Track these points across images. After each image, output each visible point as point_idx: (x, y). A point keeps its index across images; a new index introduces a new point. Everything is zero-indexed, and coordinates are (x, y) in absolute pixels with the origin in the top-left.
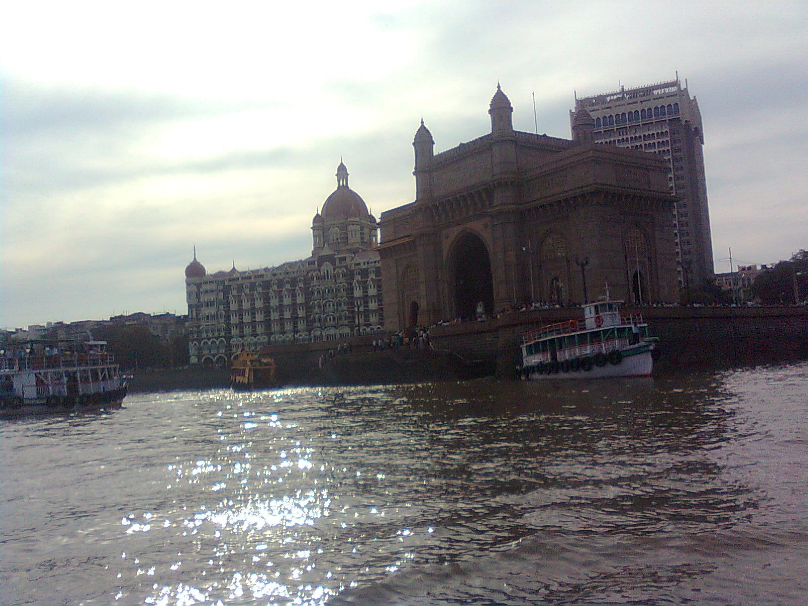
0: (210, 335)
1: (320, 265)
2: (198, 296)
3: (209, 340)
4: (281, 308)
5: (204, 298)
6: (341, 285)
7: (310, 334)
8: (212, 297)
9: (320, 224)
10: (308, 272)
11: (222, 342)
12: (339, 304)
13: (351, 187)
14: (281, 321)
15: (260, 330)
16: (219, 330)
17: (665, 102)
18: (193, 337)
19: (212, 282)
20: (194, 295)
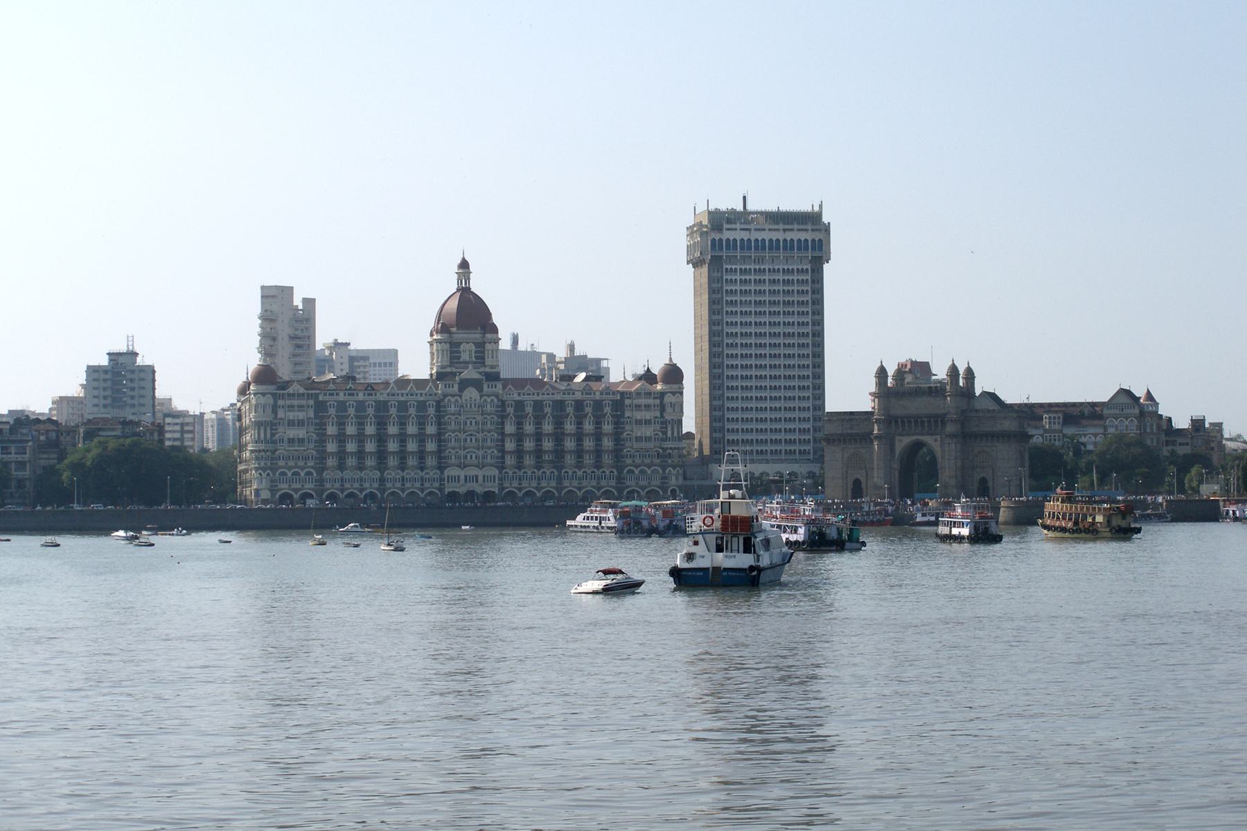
0: (291, 463)
1: (461, 389)
2: (275, 411)
3: (290, 468)
7: (442, 473)
8: (301, 415)
9: (448, 335)
10: (445, 396)
11: (309, 474)
12: (484, 440)
13: (473, 290)
14: (402, 455)
15: (370, 462)
17: (808, 236)
20: (269, 410)
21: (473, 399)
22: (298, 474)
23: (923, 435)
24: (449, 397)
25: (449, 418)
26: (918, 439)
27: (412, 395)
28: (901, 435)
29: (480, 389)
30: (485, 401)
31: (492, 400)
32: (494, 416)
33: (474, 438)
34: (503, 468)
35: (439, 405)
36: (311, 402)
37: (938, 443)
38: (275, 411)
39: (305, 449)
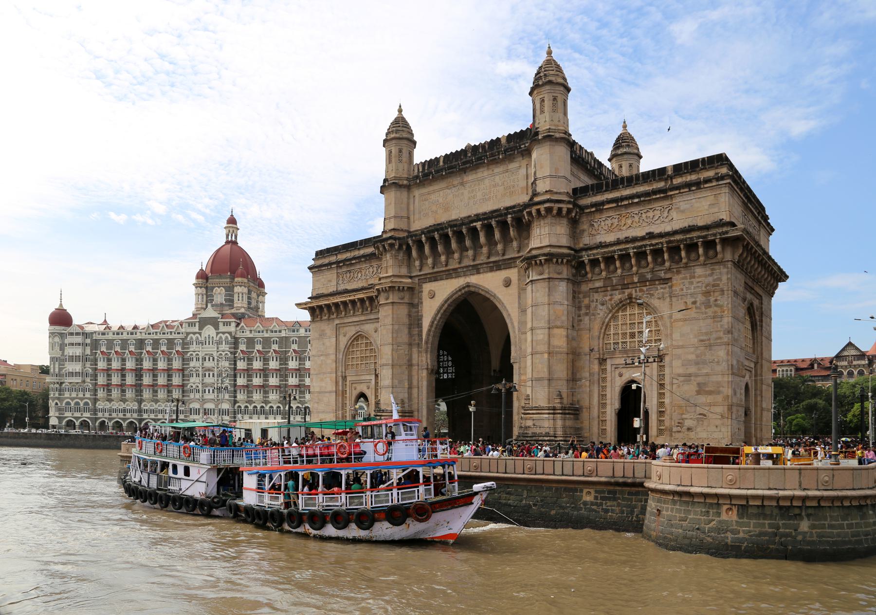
0: (74, 395)
1: (201, 328)
2: (62, 347)
4: (154, 372)
5: (70, 351)
6: (223, 354)
8: (78, 351)
10: (188, 334)
16: (84, 390)
18: (54, 394)
19: (77, 334)
20: (57, 348)
21: (211, 337)
22: (77, 404)
23: (476, 269)
24: (192, 335)
25: (192, 355)
26: (468, 285)
27: (164, 334)
28: (436, 280)
29: (216, 327)
30: (221, 338)
31: (227, 337)
32: (227, 352)
33: (211, 375)
34: (235, 402)
35: (185, 344)
36: (88, 341)
37: (514, 289)
38: (62, 347)
39: (80, 381)
